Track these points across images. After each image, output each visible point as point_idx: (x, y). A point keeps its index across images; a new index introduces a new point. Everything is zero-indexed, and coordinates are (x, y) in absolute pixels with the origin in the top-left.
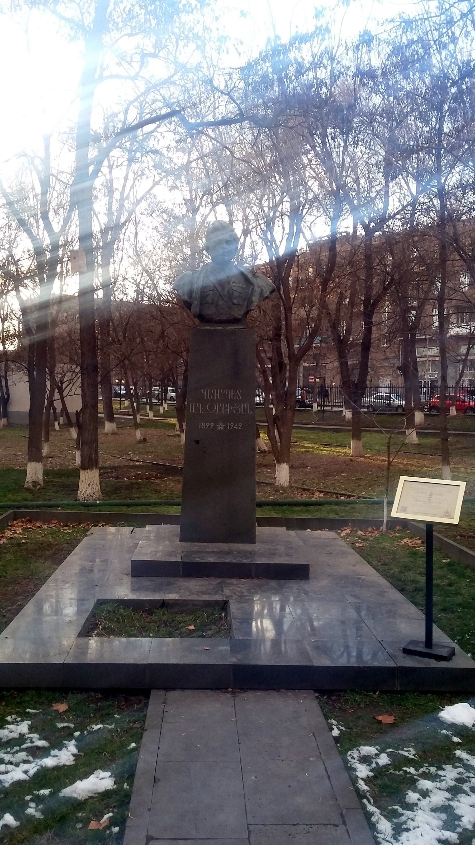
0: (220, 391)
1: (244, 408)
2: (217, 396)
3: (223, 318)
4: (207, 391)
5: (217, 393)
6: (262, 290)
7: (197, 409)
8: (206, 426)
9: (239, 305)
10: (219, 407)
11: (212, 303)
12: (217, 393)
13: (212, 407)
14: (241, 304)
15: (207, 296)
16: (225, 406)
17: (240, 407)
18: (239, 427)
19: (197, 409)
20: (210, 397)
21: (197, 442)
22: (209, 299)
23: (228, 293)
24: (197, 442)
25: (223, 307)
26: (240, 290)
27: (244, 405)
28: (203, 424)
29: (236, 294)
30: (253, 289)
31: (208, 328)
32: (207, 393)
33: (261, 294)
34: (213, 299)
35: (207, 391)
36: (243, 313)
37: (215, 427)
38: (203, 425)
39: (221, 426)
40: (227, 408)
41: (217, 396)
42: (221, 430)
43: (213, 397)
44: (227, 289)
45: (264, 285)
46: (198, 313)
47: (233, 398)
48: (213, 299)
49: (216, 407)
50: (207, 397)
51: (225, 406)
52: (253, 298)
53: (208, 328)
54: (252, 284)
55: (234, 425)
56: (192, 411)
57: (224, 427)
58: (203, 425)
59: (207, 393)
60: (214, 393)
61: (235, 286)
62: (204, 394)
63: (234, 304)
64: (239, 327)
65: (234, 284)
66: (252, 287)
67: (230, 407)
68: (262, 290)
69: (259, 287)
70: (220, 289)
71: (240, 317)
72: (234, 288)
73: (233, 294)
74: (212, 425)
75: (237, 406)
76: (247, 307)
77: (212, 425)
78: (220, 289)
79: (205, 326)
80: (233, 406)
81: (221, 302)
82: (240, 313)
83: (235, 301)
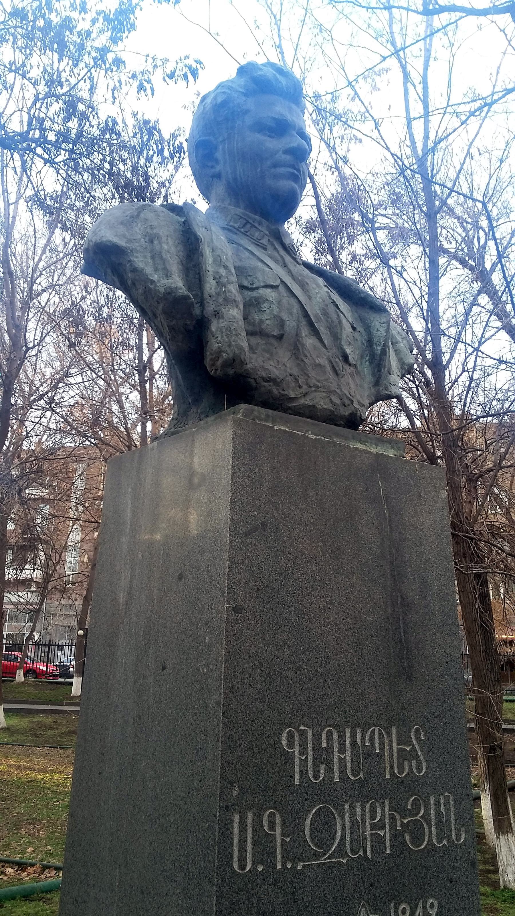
0: (353, 736)
1: (439, 814)
10: (354, 823)
11: (280, 337)
17: (426, 817)
23: (325, 313)
27: (437, 804)
34: (282, 324)
43: (330, 770)
50: (303, 774)
60: (329, 750)
62: (289, 758)
67: (393, 818)
73: (340, 322)
75: (416, 806)
76: (377, 383)
81: (309, 342)
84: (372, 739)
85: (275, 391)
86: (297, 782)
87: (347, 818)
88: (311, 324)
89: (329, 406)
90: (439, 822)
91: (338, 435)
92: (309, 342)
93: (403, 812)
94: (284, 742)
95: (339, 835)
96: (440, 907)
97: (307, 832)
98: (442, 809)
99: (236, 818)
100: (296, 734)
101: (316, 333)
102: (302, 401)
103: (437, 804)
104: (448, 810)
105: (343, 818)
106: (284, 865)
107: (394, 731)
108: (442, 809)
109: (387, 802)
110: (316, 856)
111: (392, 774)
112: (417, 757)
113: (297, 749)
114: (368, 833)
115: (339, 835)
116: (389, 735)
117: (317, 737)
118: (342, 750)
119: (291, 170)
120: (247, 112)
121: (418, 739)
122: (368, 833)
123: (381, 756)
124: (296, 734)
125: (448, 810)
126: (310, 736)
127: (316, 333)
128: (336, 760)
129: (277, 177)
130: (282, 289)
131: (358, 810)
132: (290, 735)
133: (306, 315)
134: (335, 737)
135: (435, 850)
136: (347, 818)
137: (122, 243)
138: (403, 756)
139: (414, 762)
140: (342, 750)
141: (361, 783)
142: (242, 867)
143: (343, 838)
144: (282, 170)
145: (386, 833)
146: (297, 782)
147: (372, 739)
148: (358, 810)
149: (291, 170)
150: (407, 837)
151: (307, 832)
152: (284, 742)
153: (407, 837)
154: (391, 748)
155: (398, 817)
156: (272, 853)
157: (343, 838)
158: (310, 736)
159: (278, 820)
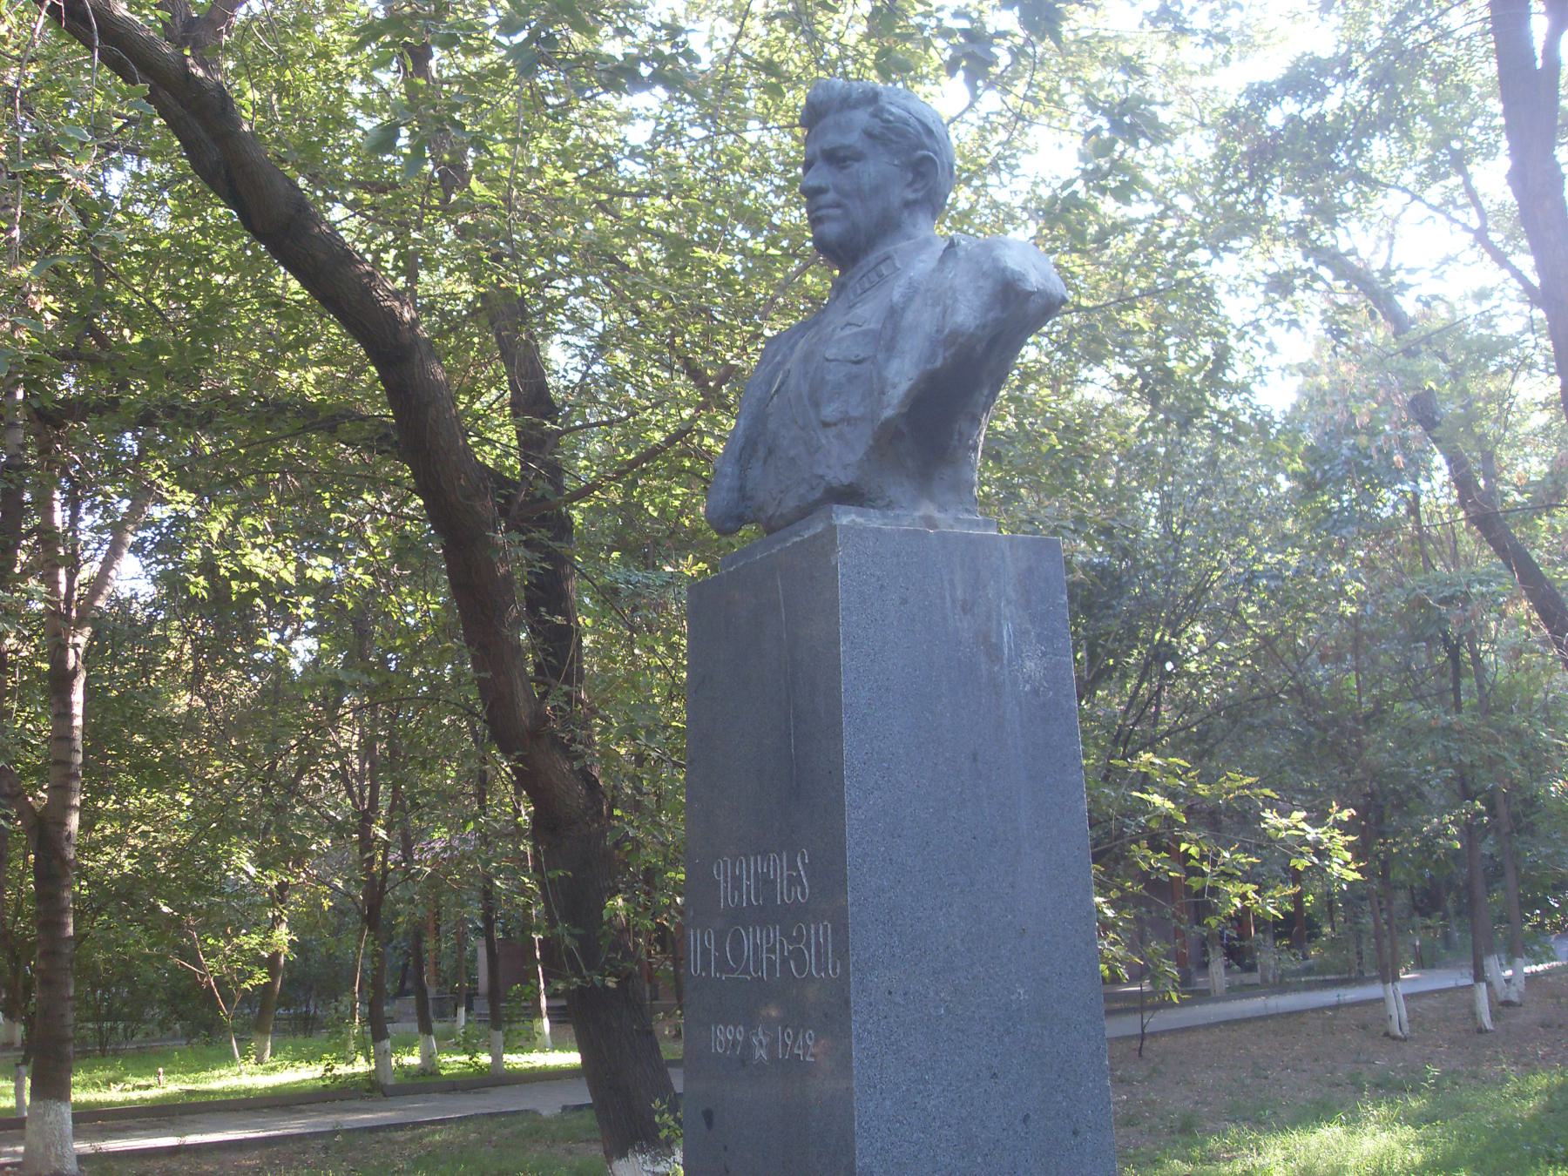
1: (818, 943)
9: (847, 419)
10: (755, 944)
35: (725, 863)
37: (748, 1045)
43: (741, 896)
63: (826, 425)
90: (818, 952)
93: (791, 940)
104: (826, 940)
110: (733, 971)
112: (802, 884)
118: (748, 878)
123: (774, 881)
125: (826, 940)
140: (748, 878)
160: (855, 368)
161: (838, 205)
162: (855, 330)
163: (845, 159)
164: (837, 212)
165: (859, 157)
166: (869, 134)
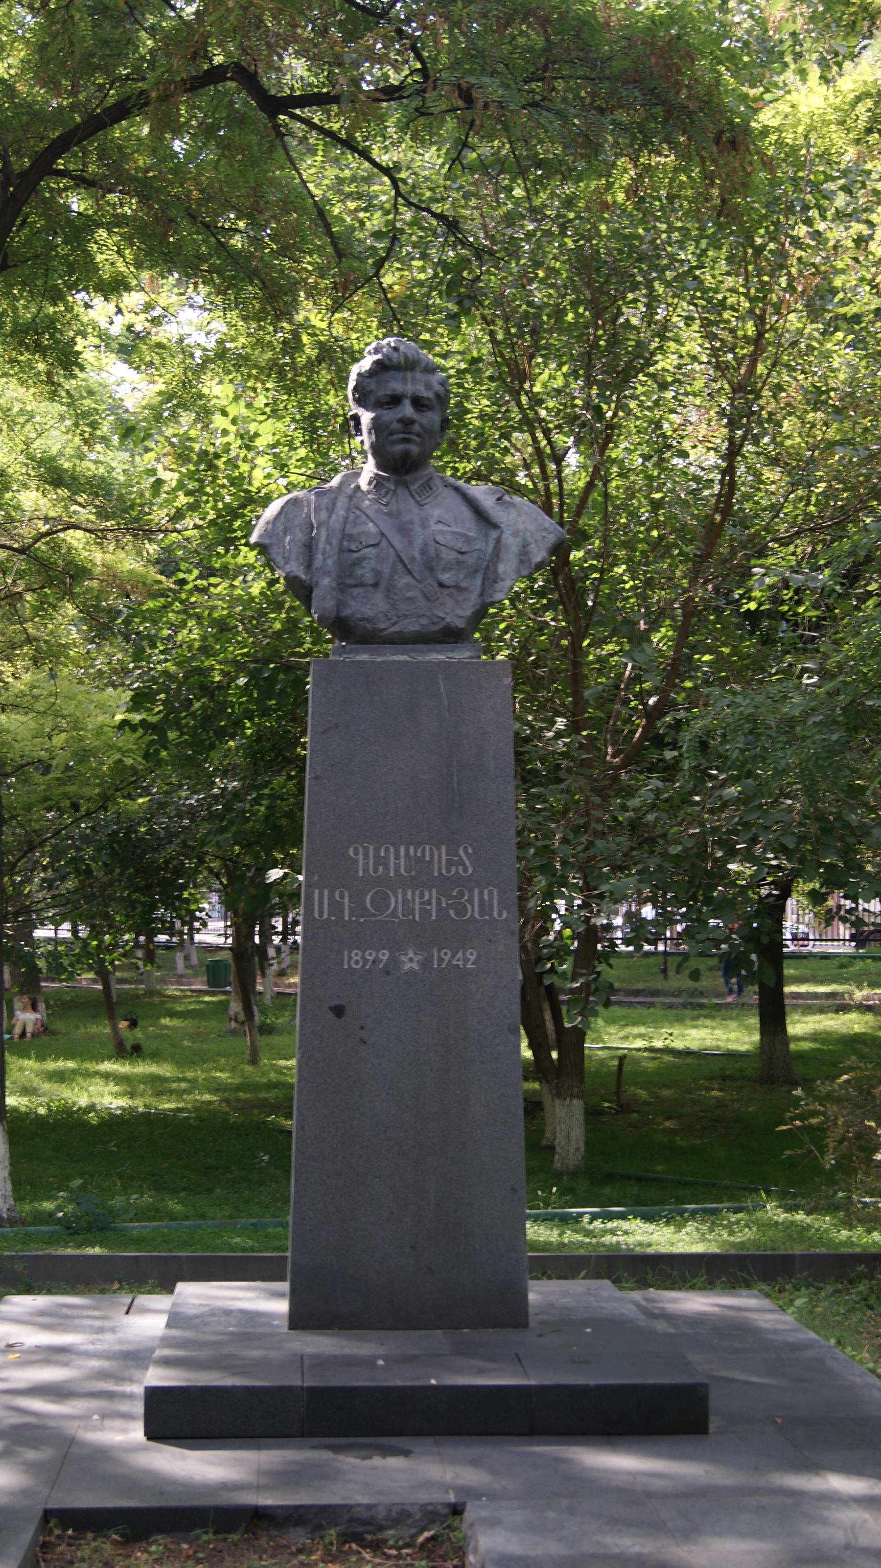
1: (481, 900)
2: (397, 866)
3: (411, 626)
4: (366, 849)
5: (397, 857)
6: (525, 545)
7: (336, 907)
8: (366, 961)
9: (457, 587)
10: (405, 901)
11: (376, 585)
12: (397, 857)
13: (381, 901)
14: (464, 584)
15: (358, 562)
16: (422, 896)
17: (471, 901)
18: (466, 961)
19: (336, 907)
20: (376, 871)
21: (339, 1011)
22: (365, 573)
23: (423, 552)
24: (339, 1011)
25: (410, 594)
26: (460, 545)
27: (481, 894)
28: (356, 955)
29: (448, 556)
30: (498, 540)
31: (364, 657)
32: (366, 856)
33: (524, 553)
34: (377, 573)
36: (468, 612)
37: (394, 962)
38: (354, 959)
39: (411, 961)
40: (429, 903)
41: (397, 866)
42: (411, 971)
43: (387, 868)
44: (418, 542)
45: (532, 528)
46: (333, 615)
47: (448, 871)
48: (377, 573)
49: (395, 902)
50: (366, 870)
51: (422, 896)
52: (501, 568)
53: (364, 657)
54: (495, 526)
55: (454, 955)
56: (321, 914)
57: (422, 964)
58: (354, 959)
59: (366, 856)
60: (387, 858)
61: (442, 532)
62: (355, 862)
63: (441, 585)
64: (461, 654)
65: (441, 527)
66: (494, 534)
67: (439, 901)
68: (525, 545)
69: (515, 534)
70: (397, 541)
71: (460, 624)
72: (440, 538)
73: (437, 556)
74: (385, 956)
76: (482, 594)
77: (385, 956)
78: (397, 541)
79: (357, 652)
80: (449, 897)
82: (460, 612)
83: (445, 577)
84: (423, 852)
85: (369, 626)
86: (361, 873)
87: (400, 897)
88: (405, 566)
89: (417, 628)
91: (414, 651)
92: (404, 580)
94: (351, 852)
95: (393, 905)
96: (479, 955)
97: (368, 902)
98: (486, 897)
99: (317, 892)
100: (361, 849)
101: (410, 572)
102: (392, 630)
103: (481, 894)
105: (396, 897)
106: (350, 916)
107: (444, 849)
108: (486, 897)
109: (434, 891)
110: (374, 915)
111: (440, 873)
112: (463, 864)
113: (361, 857)
114: (417, 906)
115: (393, 905)
116: (439, 850)
117: (376, 850)
119: (401, 436)
120: (371, 392)
121: (466, 853)
122: (417, 906)
123: (431, 862)
124: (361, 849)
126: (371, 848)
127: (410, 572)
128: (392, 864)
129: (393, 443)
130: (384, 544)
131: (409, 893)
132: (356, 850)
133: (402, 561)
134: (392, 850)
135: (476, 921)
136: (400, 897)
137: (267, 541)
138: (450, 863)
139: (461, 868)
141: (413, 878)
142: (321, 916)
143: (396, 907)
144: (395, 437)
145: (434, 907)
146: (361, 873)
147: (423, 852)
148: (409, 893)
149: (401, 436)
150: (452, 912)
151: (368, 902)
152: (351, 852)
153: (452, 912)
154: (440, 858)
155: (444, 900)
156: (342, 911)
157: (396, 907)
158: (371, 848)
159: (346, 895)
160: (460, 556)
161: (418, 435)
162: (446, 528)
163: (423, 406)
164: (418, 439)
165: (430, 408)
166: (438, 396)
